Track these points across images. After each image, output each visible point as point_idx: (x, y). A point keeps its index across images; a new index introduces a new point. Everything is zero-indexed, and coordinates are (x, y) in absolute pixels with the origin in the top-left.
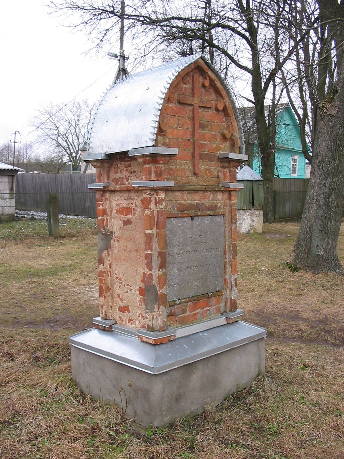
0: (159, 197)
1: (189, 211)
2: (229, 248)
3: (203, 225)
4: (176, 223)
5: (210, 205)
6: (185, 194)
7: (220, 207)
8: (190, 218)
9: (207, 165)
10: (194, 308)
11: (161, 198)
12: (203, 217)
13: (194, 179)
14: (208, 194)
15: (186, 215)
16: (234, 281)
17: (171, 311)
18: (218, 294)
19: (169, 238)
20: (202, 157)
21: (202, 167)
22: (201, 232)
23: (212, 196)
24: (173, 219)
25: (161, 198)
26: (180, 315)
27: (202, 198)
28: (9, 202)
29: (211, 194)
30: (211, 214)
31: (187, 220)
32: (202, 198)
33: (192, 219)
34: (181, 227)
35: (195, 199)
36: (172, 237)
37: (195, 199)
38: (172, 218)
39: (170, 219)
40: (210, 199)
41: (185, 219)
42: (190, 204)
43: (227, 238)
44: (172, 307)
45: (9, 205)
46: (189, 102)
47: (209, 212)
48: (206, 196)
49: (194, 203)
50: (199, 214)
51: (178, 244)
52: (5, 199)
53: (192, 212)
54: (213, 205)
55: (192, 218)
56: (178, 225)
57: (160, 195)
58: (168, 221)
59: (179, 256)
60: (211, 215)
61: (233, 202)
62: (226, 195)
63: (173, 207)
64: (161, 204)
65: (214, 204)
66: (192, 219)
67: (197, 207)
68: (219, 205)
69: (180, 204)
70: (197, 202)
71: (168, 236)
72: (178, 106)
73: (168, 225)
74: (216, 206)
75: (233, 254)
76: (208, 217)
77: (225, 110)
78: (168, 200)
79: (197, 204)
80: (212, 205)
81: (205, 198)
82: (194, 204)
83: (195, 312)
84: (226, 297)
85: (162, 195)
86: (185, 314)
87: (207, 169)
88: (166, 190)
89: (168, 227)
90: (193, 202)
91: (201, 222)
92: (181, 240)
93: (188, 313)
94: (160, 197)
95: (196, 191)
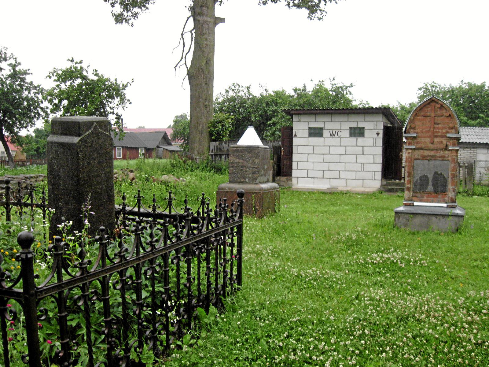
10: (428, 196)
14: (439, 151)
20: (436, 136)
21: (437, 140)
23: (442, 152)
31: (426, 162)
35: (431, 153)
37: (431, 153)
40: (442, 153)
47: (439, 159)
53: (428, 158)
55: (429, 161)
62: (450, 152)
63: (418, 156)
67: (432, 156)
72: (422, 117)
77: (450, 115)
85: (410, 151)
88: (411, 149)
95: (432, 150)
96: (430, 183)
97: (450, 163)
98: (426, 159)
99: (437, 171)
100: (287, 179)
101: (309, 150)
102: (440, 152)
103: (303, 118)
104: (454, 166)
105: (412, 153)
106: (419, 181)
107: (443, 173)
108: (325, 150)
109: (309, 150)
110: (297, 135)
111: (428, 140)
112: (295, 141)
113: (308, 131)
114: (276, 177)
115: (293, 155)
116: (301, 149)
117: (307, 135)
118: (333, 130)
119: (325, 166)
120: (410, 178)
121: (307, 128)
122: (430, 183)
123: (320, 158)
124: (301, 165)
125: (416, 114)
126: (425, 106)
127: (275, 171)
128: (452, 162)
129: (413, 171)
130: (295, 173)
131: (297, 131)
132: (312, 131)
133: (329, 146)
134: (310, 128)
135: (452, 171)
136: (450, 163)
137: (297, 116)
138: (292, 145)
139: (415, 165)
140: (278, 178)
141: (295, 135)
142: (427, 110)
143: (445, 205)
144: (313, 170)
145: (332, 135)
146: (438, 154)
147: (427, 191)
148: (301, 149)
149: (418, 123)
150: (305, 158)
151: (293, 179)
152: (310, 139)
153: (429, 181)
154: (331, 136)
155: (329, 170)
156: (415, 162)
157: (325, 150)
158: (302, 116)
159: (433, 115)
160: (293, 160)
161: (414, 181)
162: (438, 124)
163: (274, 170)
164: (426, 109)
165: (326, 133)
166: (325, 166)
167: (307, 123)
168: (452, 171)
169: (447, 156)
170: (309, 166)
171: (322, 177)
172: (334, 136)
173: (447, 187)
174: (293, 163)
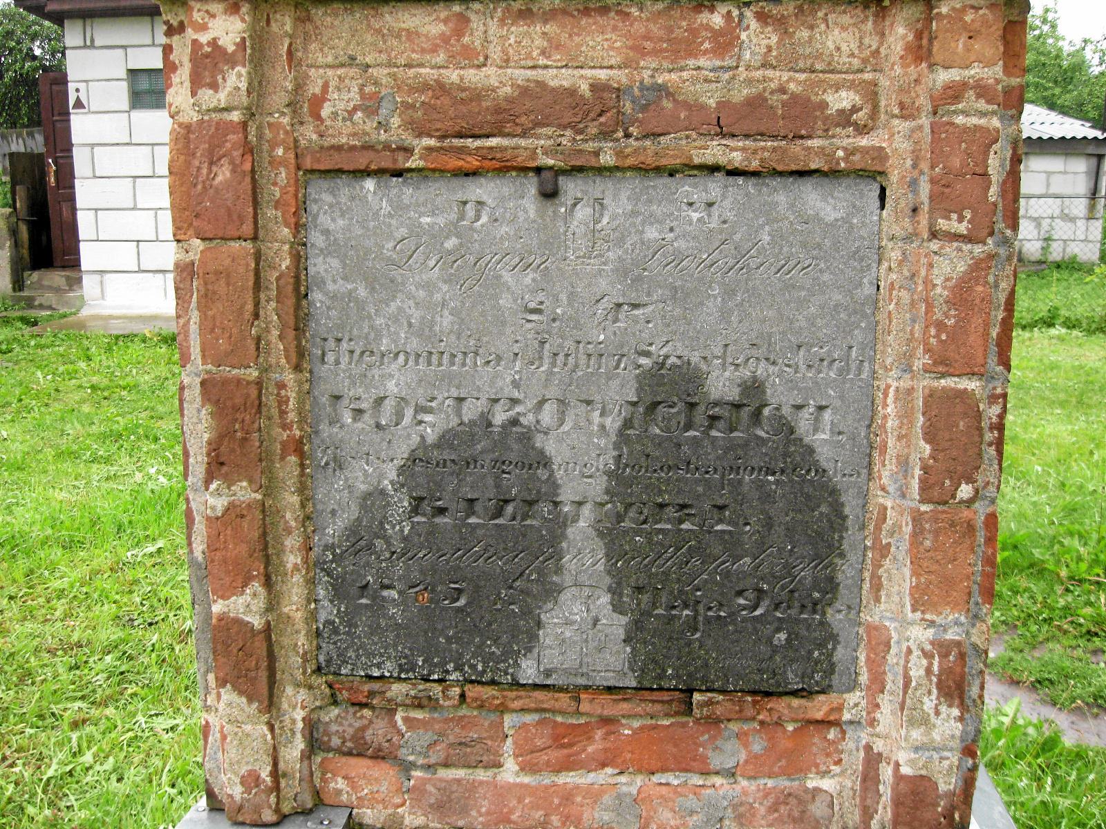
0: (195, 42)
1: (524, 135)
2: (906, 416)
3: (652, 233)
4: (399, 208)
5: (740, 94)
6: (476, 23)
7: (844, 118)
8: (531, 186)
11: (214, 43)
12: (667, 180)
15: (474, 163)
16: (928, 655)
17: (363, 729)
19: (334, 297)
22: (638, 279)
24: (370, 184)
25: (214, 43)
26: (446, 765)
27: (656, 53)
28: (1084, 228)
29: (754, 24)
30: (737, 159)
32: (648, 45)
33: (550, 194)
34: (437, 236)
36: (362, 292)
38: (366, 173)
39: (342, 181)
42: (533, 92)
43: (892, 347)
44: (367, 712)
45: (1083, 237)
47: (714, 151)
48: (694, 32)
49: (581, 80)
50: (607, 159)
51: (414, 344)
52: (1073, 220)
54: (775, 100)
56: (416, 231)
57: (203, 28)
58: (327, 197)
59: (428, 418)
60: (755, 174)
61: (944, 76)
63: (370, 105)
64: (214, 86)
65: (782, 90)
66: (550, 194)
69: (441, 88)
70: (602, 74)
71: (331, 287)
73: (324, 220)
75: (925, 469)
76: (715, 187)
78: (330, 59)
79: (596, 87)
80: (756, 103)
81: (685, 48)
82: (572, 92)
83: (568, 779)
84: (868, 748)
86: (482, 775)
89: (326, 232)
91: (634, 213)
92: (446, 321)
93: (510, 772)
94: (204, 38)
96: (582, 529)
97: (893, 222)
98: (504, 167)
99: (674, 350)
100: (68, 278)
102: (725, 42)
103: (106, 33)
104: (980, 267)
106: (399, 524)
107: (779, 396)
110: (85, 102)
112: (81, 127)
113: (125, 85)
114: (26, 274)
115: (77, 183)
116: (107, 161)
117: (124, 104)
120: (244, 492)
121: (123, 75)
122: (582, 529)
124: (111, 224)
127: (25, 252)
128: (943, 201)
129: (300, 359)
130: (89, 256)
131: (82, 86)
132: (144, 84)
134: (133, 73)
135: (942, 364)
136: (893, 222)
137: (79, 23)
138: (68, 148)
139: (319, 266)
140: (36, 275)
141: (79, 104)
147: (529, 671)
148: (107, 161)
150: (120, 192)
151: (86, 280)
152: (138, 115)
153: (559, 525)
158: (96, 20)
160: (78, 205)
161: (333, 530)
163: (16, 245)
167: (120, 52)
168: (942, 364)
169: (841, 100)
173: (836, 617)
174: (80, 215)
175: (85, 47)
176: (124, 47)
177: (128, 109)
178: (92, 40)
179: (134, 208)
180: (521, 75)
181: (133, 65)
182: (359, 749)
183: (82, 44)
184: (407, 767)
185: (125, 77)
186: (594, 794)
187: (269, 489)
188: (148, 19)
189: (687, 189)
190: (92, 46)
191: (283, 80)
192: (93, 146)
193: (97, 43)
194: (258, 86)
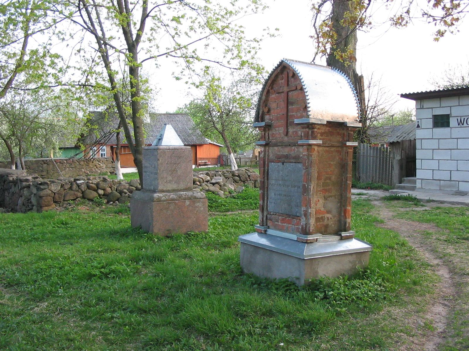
9: (294, 128)
10: (283, 221)
13: (286, 138)
14: (293, 148)
18: (297, 217)
30: (294, 161)
41: (280, 164)
46: (281, 91)
47: (291, 161)
49: (285, 154)
67: (287, 157)
68: (301, 156)
72: (277, 95)
74: (299, 156)
80: (296, 156)
81: (291, 151)
87: (294, 132)
90: (284, 154)
92: (277, 176)
101: (434, 144)
102: (294, 150)
105: (265, 151)
108: (452, 144)
109: (434, 144)
110: (420, 126)
111: (282, 130)
113: (432, 119)
117: (431, 126)
118: (461, 117)
119: (452, 165)
123: (446, 155)
125: (268, 92)
126: (277, 76)
133: (457, 139)
139: (270, 171)
142: (282, 83)
143: (294, 237)
144: (439, 170)
145: (460, 123)
146: (293, 154)
148: (426, 144)
149: (273, 105)
154: (459, 125)
155: (457, 170)
156: (272, 165)
157: (452, 144)
158: (424, 100)
159: (286, 89)
162: (292, 104)
164: (280, 81)
165: (453, 122)
166: (452, 165)
169: (301, 156)
170: (434, 165)
171: (449, 179)
172: (463, 124)
175: (421, 108)
176: (432, 108)
177: (432, 127)
178: (423, 106)
179: (433, 159)
180: (282, 153)
181: (434, 114)
182: (270, 220)
183: (420, 107)
184: (273, 222)
185: (431, 117)
186: (285, 226)
187: (264, 191)
188: (439, 99)
189: (291, 164)
190: (423, 108)
191: (267, 153)
192: (422, 139)
193: (424, 107)
194: (265, 154)
